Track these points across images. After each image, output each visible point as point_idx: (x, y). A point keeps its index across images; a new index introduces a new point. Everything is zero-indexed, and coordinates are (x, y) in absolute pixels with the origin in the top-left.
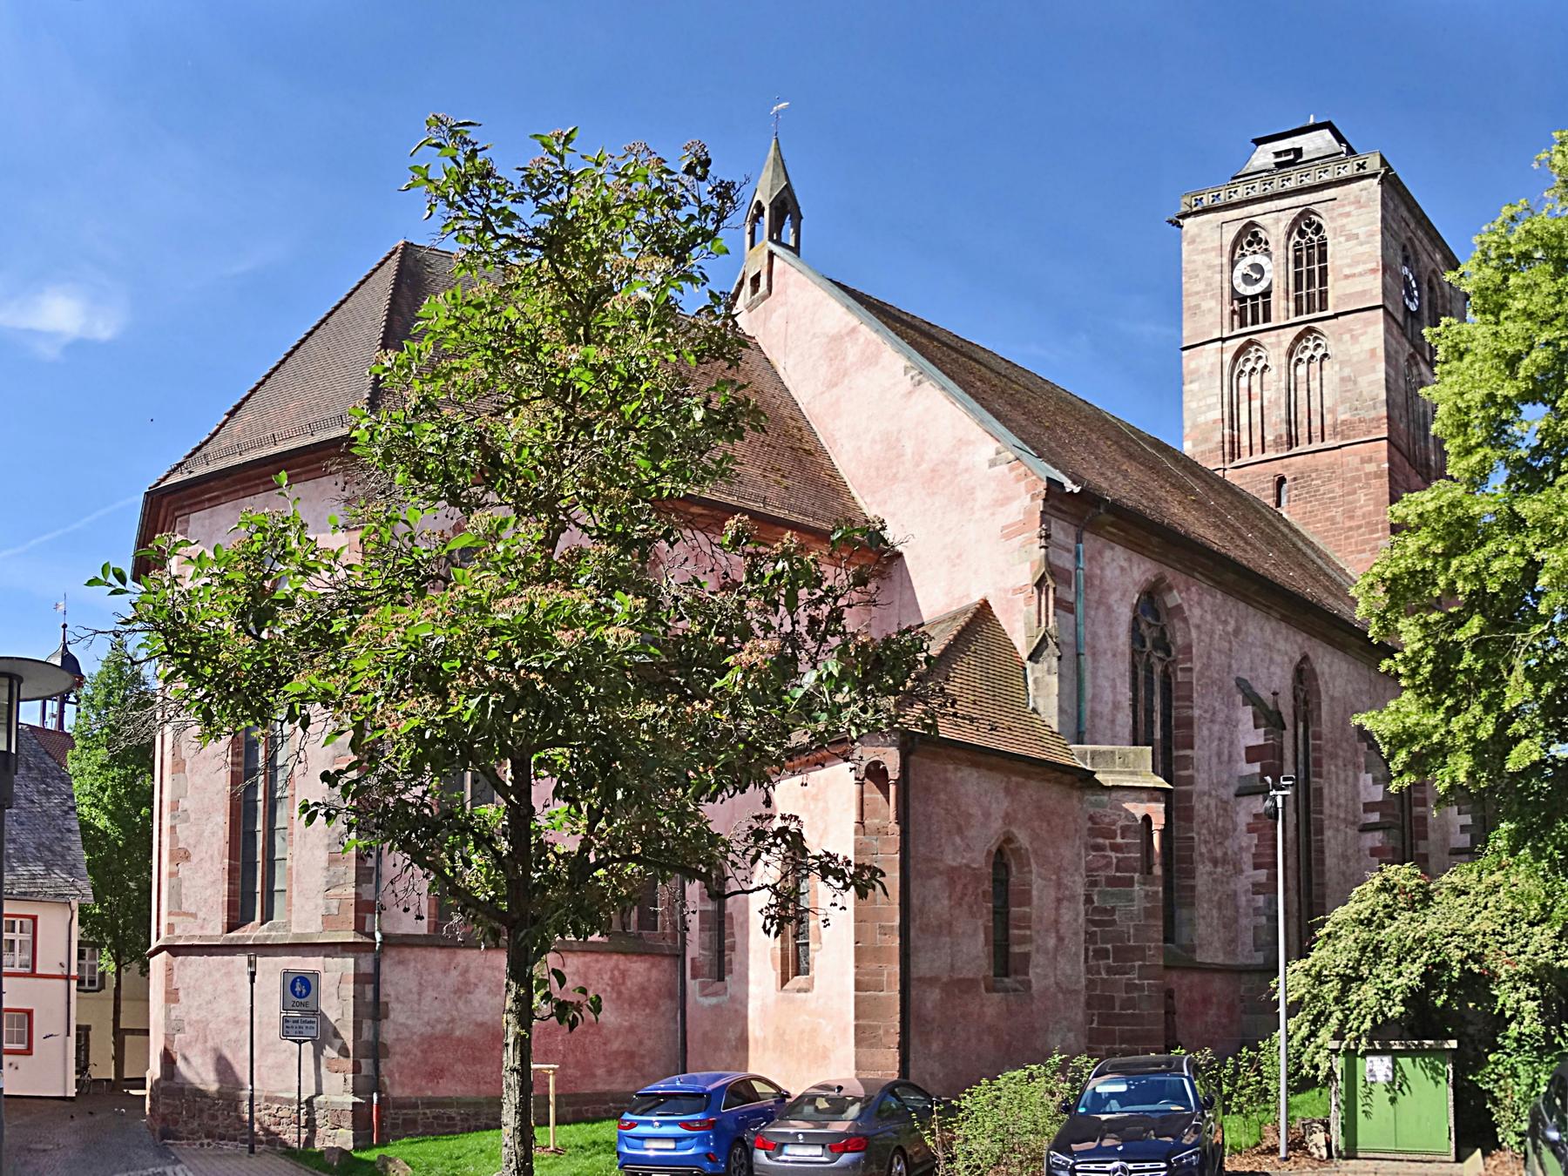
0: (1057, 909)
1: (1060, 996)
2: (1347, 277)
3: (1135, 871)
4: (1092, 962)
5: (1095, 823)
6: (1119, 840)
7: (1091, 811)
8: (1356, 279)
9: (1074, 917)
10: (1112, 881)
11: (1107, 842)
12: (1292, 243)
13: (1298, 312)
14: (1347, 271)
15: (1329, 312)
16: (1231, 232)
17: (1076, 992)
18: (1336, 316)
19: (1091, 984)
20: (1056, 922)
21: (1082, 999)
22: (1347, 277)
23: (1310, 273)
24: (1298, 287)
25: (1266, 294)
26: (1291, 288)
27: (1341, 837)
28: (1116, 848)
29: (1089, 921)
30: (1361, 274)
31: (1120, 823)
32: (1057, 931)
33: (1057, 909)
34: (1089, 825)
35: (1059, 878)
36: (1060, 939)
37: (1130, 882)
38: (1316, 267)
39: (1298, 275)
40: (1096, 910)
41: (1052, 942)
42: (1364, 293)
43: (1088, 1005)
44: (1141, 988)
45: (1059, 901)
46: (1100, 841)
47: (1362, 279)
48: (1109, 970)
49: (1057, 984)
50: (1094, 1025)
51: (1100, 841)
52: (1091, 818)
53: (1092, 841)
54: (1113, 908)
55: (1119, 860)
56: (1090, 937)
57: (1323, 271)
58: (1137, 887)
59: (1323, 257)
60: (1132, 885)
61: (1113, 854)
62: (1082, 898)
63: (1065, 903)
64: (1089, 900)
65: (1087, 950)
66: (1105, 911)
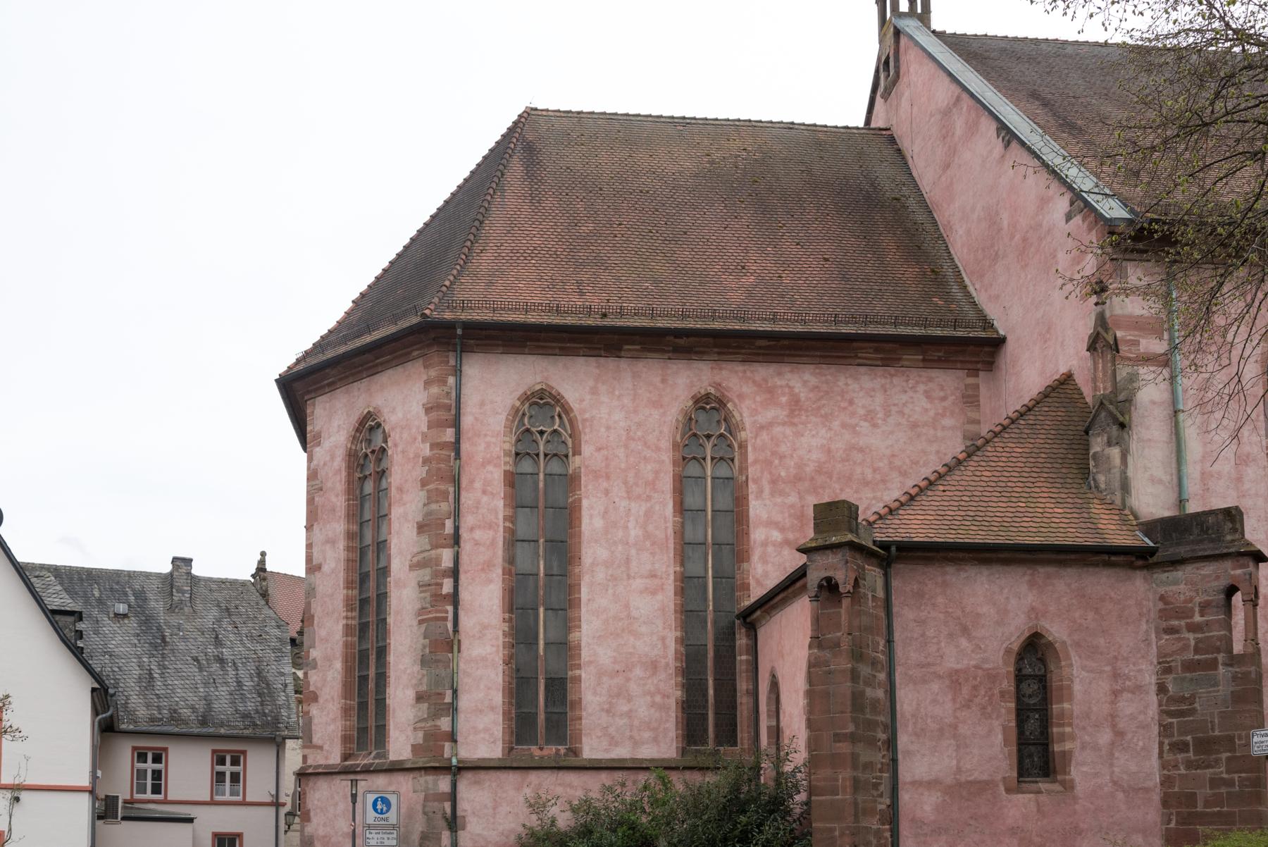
0: (1113, 703)
1: (1120, 795)
3: (1218, 651)
4: (1167, 756)
5: (1166, 603)
6: (1197, 618)
7: (1162, 590)
9: (1143, 710)
10: (1189, 666)
11: (1183, 623)
17: (1147, 790)
19: (1166, 781)
20: (1113, 716)
21: (1156, 797)
28: (1193, 628)
29: (1162, 712)
31: (1198, 600)
32: (1114, 726)
33: (1113, 703)
34: (1161, 605)
35: (1114, 669)
36: (1120, 734)
37: (1213, 665)
40: (1172, 700)
41: (1105, 737)
43: (1165, 803)
44: (1230, 783)
45: (1116, 694)
46: (1176, 623)
48: (1189, 765)
49: (1115, 783)
50: (1172, 825)
51: (1176, 623)
52: (1162, 598)
53: (1164, 624)
54: (1193, 697)
55: (1198, 641)
56: (1165, 730)
58: (1221, 669)
60: (1216, 668)
61: (1191, 636)
62: (1154, 688)
63: (1126, 695)
64: (1161, 689)
65: (1161, 744)
66: (1182, 700)
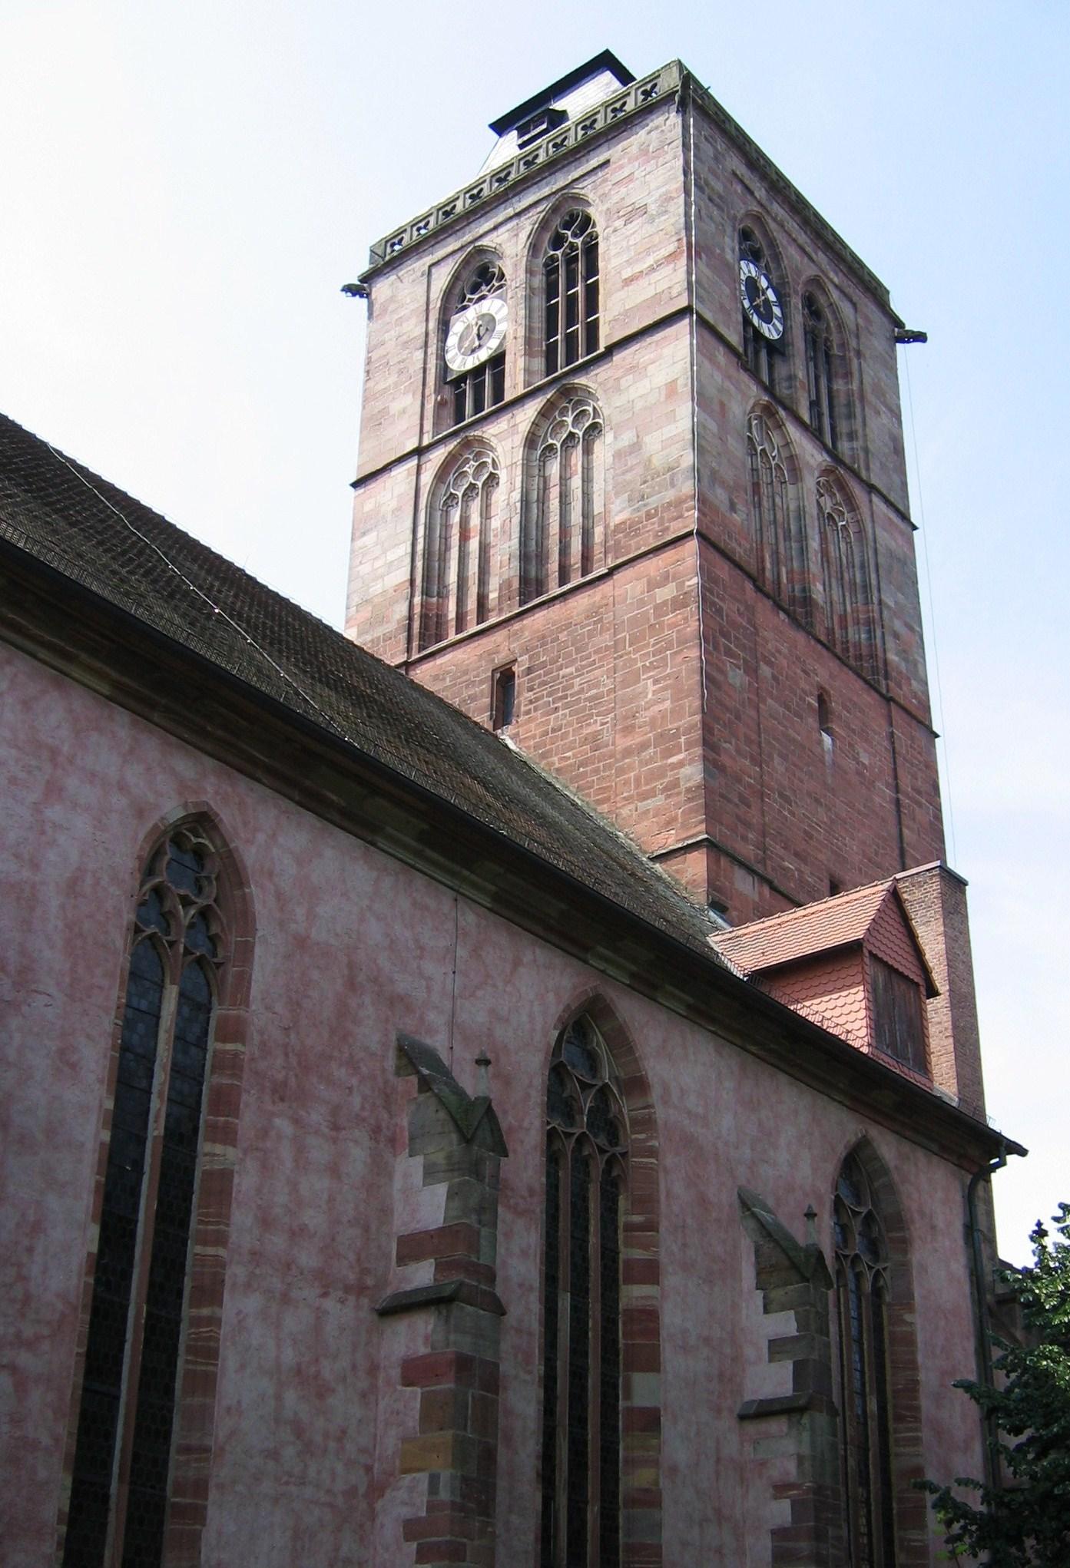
2: (628, 281)
8: (643, 282)
12: (541, 260)
13: (551, 367)
14: (627, 273)
15: (602, 349)
16: (442, 278)
18: (611, 350)
22: (628, 281)
23: (571, 301)
24: (551, 330)
25: (498, 361)
26: (539, 335)
27: (294, 1322)
30: (652, 269)
38: (579, 289)
39: (551, 312)
42: (657, 298)
47: (655, 276)
57: (592, 291)
59: (592, 269)
